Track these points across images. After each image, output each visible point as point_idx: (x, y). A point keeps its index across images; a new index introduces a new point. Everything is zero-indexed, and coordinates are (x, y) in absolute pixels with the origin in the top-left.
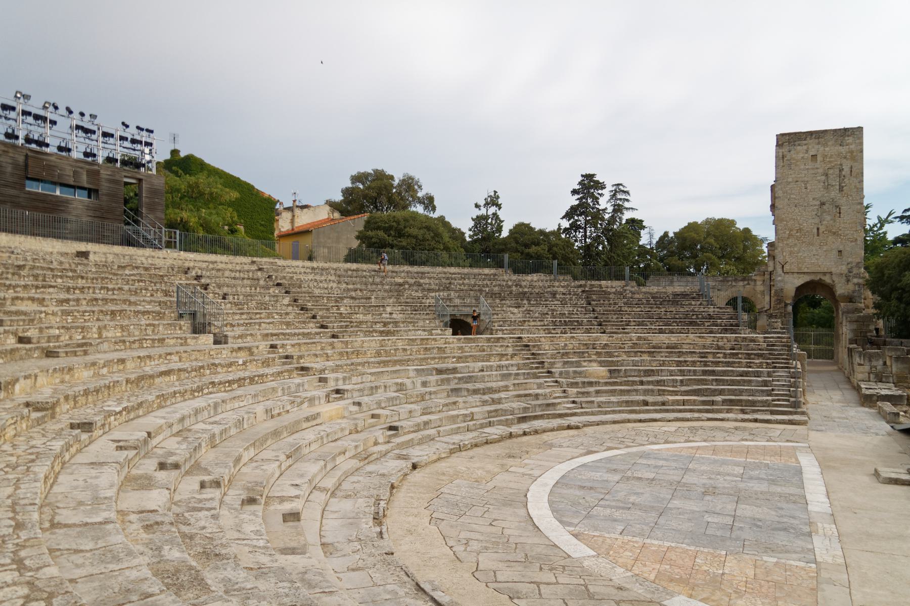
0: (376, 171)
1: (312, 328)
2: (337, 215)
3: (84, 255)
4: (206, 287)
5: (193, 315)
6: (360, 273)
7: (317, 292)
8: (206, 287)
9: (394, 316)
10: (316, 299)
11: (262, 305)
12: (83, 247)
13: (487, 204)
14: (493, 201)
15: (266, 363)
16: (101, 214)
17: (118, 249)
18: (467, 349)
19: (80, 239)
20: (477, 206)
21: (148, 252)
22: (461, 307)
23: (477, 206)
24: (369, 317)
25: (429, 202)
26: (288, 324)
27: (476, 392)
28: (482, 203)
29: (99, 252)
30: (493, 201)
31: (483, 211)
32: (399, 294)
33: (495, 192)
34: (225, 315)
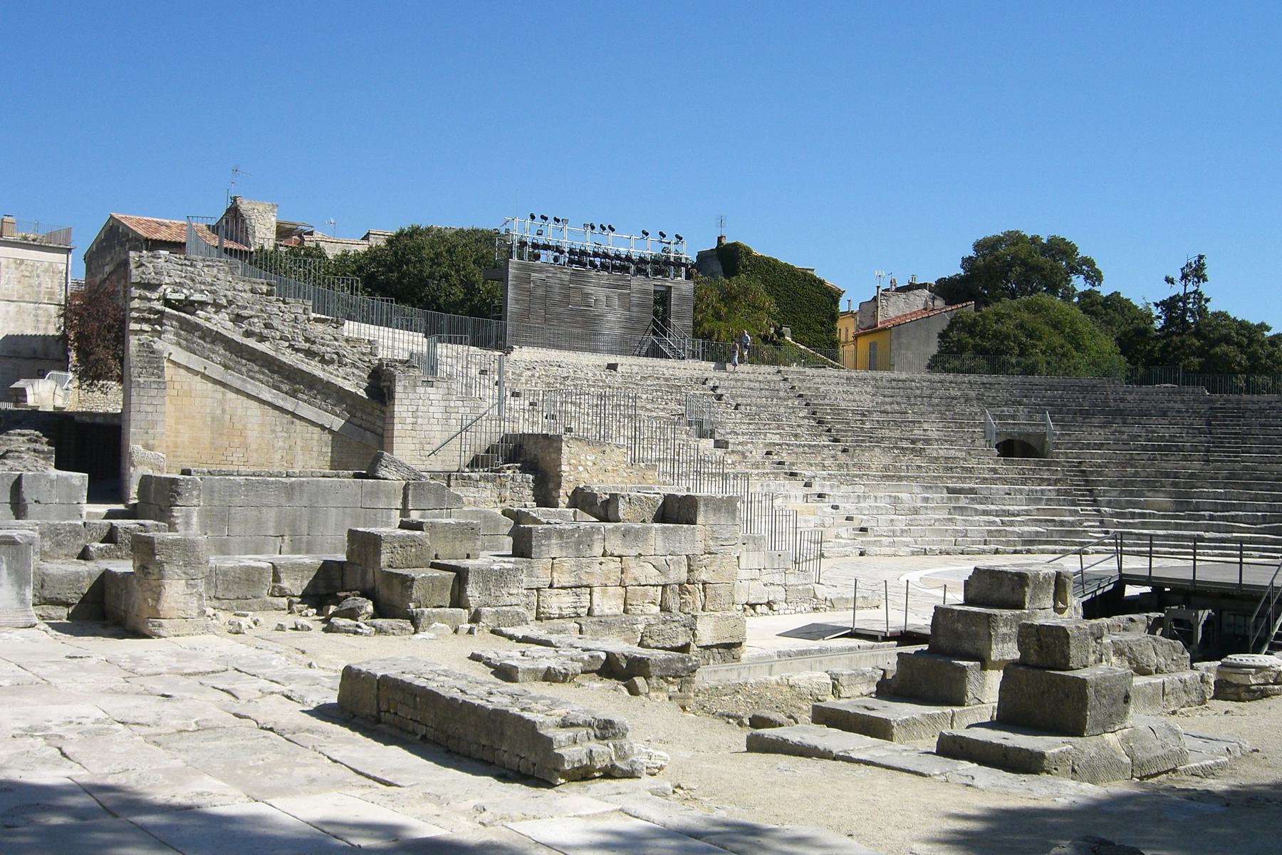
0: (1009, 234)
1: (824, 440)
2: (939, 303)
3: (612, 367)
4: (719, 397)
5: (700, 424)
6: (907, 384)
7: (843, 405)
8: (719, 397)
9: (929, 433)
10: (836, 411)
11: (776, 417)
12: (612, 359)
13: (1184, 277)
14: (1196, 271)
15: (756, 465)
16: (631, 324)
17: (643, 361)
18: (1000, 471)
19: (611, 352)
20: (1170, 281)
21: (671, 362)
22: (1021, 423)
23: (1170, 281)
24: (897, 434)
25: (1095, 276)
26: (796, 436)
27: (985, 513)
28: (1177, 276)
29: (627, 363)
30: (1196, 271)
31: (1178, 289)
32: (949, 407)
33: (1201, 257)
34: (731, 423)
